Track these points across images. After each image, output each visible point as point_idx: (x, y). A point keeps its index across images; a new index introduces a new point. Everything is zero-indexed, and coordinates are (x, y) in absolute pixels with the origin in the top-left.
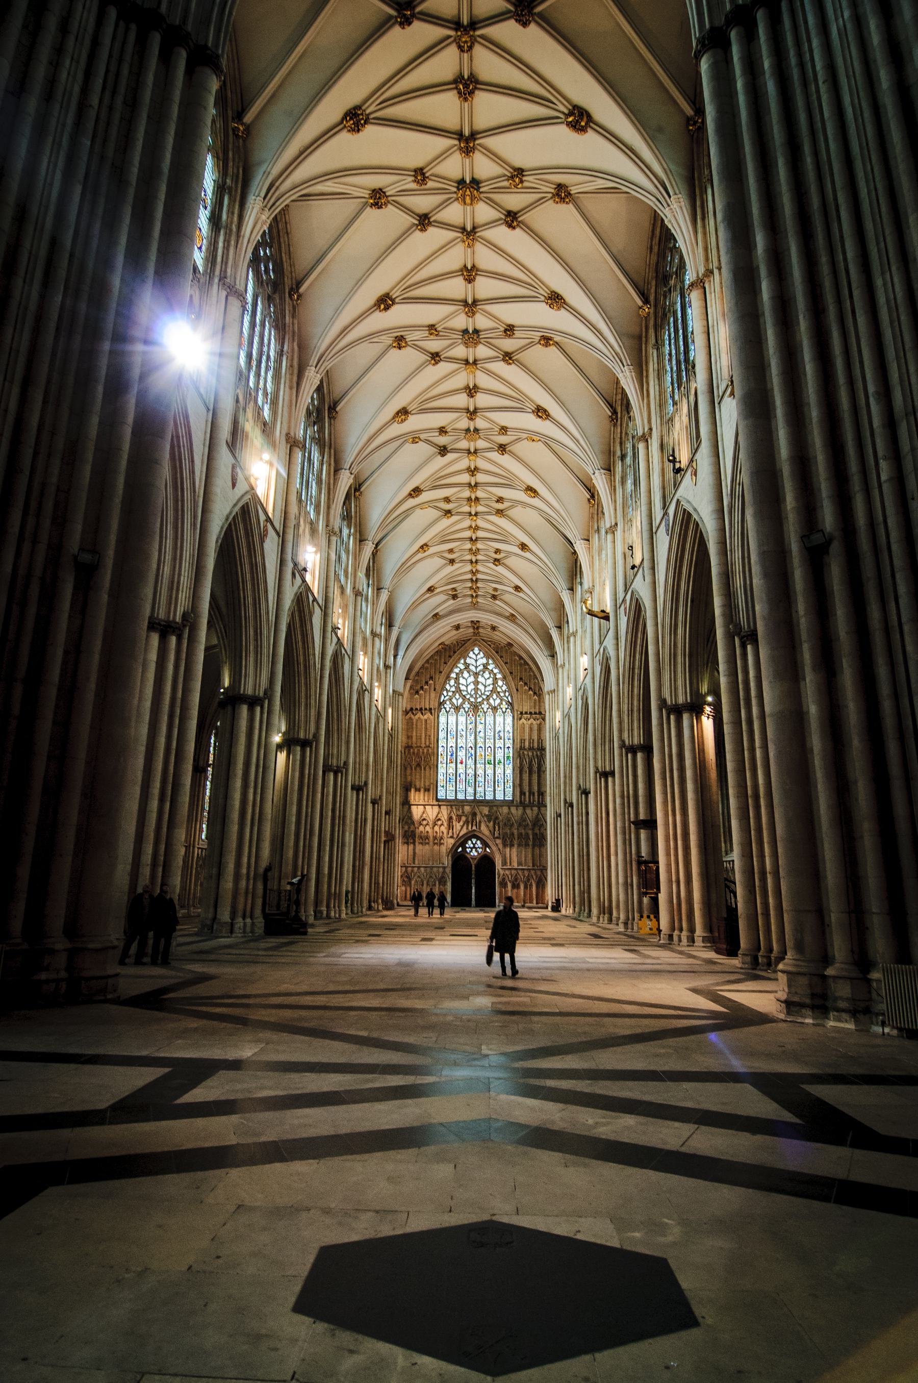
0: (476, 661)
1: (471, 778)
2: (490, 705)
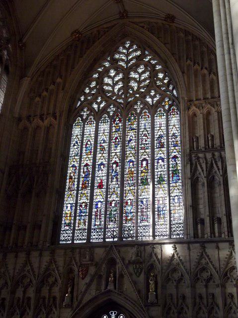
0: (127, 55)
1: (114, 210)
2: (146, 104)
